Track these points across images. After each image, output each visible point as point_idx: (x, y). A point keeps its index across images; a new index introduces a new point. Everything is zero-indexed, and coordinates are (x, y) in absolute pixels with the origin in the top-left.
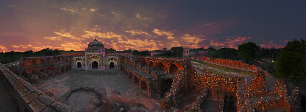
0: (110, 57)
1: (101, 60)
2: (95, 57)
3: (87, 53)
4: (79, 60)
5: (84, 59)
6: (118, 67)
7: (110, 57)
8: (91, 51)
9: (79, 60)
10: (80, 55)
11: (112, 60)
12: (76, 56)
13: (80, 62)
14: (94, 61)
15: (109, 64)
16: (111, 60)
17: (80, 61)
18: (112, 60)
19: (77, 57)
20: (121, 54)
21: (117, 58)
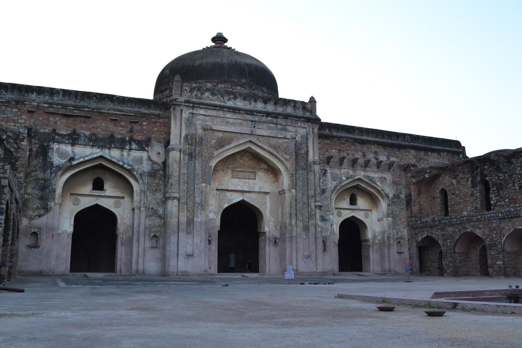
0: (345, 174)
1: (294, 185)
2: (252, 159)
3: (190, 123)
4: (98, 185)
5: (161, 173)
6: (394, 249)
7: (345, 174)
8: (222, 108)
9: (98, 185)
10: (120, 131)
11: (353, 201)
12: (74, 139)
13: (107, 204)
14: (237, 198)
15: (336, 229)
16: (345, 203)
17: (110, 189)
18: (353, 201)
19: (96, 152)
20: (410, 157)
21: (385, 182)
